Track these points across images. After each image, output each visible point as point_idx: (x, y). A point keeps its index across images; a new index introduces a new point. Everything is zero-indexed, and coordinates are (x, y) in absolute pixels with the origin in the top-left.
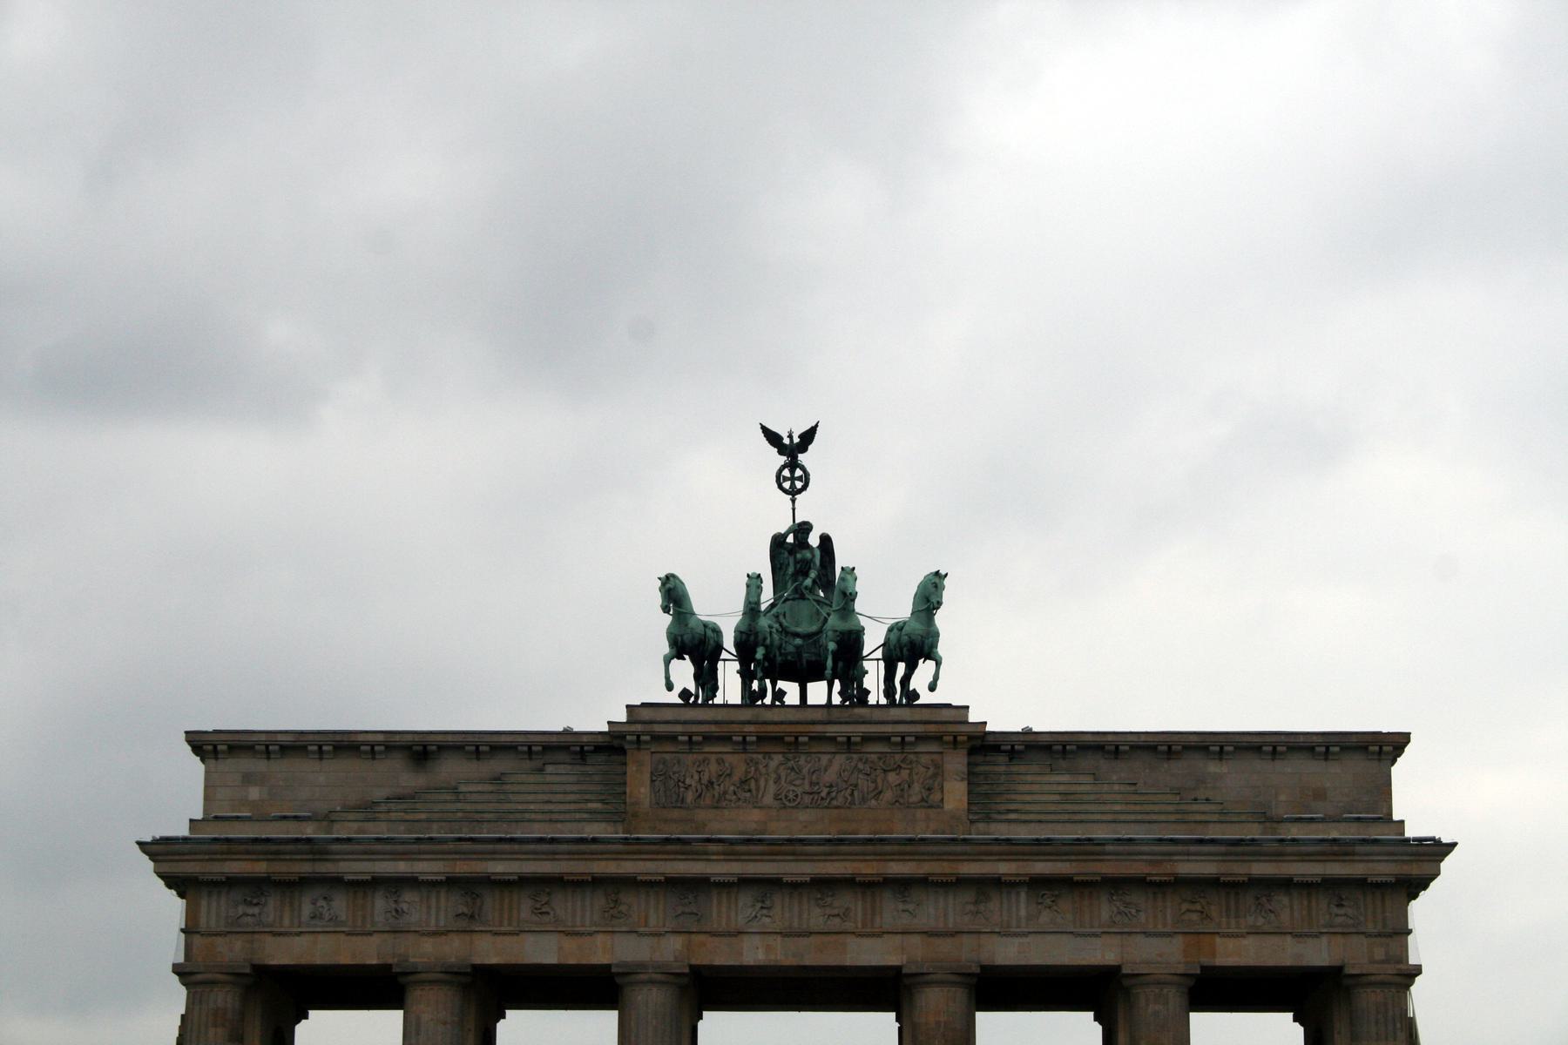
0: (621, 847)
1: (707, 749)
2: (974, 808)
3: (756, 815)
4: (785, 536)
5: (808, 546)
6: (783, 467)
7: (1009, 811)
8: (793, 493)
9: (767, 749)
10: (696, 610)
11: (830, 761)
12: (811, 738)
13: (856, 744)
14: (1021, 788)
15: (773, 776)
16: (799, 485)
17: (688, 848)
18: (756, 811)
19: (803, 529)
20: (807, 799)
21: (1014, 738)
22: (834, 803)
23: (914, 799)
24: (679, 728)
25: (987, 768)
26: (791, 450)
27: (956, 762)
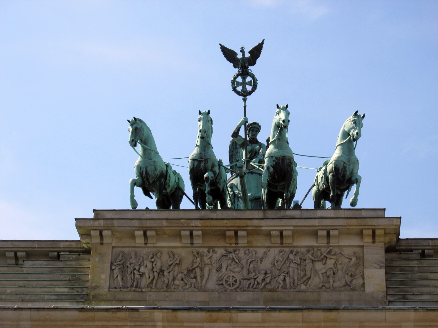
0: (77, 313)
2: (391, 292)
3: (201, 296)
4: (238, 129)
5: (256, 142)
6: (238, 75)
7: (422, 294)
8: (245, 94)
9: (212, 244)
10: (159, 150)
11: (265, 253)
13: (288, 236)
14: (432, 276)
15: (217, 265)
16: (249, 88)
17: (135, 314)
18: (199, 293)
19: (254, 128)
21: (425, 243)
22: (268, 287)
24: (136, 223)
26: (244, 63)
27: (375, 253)
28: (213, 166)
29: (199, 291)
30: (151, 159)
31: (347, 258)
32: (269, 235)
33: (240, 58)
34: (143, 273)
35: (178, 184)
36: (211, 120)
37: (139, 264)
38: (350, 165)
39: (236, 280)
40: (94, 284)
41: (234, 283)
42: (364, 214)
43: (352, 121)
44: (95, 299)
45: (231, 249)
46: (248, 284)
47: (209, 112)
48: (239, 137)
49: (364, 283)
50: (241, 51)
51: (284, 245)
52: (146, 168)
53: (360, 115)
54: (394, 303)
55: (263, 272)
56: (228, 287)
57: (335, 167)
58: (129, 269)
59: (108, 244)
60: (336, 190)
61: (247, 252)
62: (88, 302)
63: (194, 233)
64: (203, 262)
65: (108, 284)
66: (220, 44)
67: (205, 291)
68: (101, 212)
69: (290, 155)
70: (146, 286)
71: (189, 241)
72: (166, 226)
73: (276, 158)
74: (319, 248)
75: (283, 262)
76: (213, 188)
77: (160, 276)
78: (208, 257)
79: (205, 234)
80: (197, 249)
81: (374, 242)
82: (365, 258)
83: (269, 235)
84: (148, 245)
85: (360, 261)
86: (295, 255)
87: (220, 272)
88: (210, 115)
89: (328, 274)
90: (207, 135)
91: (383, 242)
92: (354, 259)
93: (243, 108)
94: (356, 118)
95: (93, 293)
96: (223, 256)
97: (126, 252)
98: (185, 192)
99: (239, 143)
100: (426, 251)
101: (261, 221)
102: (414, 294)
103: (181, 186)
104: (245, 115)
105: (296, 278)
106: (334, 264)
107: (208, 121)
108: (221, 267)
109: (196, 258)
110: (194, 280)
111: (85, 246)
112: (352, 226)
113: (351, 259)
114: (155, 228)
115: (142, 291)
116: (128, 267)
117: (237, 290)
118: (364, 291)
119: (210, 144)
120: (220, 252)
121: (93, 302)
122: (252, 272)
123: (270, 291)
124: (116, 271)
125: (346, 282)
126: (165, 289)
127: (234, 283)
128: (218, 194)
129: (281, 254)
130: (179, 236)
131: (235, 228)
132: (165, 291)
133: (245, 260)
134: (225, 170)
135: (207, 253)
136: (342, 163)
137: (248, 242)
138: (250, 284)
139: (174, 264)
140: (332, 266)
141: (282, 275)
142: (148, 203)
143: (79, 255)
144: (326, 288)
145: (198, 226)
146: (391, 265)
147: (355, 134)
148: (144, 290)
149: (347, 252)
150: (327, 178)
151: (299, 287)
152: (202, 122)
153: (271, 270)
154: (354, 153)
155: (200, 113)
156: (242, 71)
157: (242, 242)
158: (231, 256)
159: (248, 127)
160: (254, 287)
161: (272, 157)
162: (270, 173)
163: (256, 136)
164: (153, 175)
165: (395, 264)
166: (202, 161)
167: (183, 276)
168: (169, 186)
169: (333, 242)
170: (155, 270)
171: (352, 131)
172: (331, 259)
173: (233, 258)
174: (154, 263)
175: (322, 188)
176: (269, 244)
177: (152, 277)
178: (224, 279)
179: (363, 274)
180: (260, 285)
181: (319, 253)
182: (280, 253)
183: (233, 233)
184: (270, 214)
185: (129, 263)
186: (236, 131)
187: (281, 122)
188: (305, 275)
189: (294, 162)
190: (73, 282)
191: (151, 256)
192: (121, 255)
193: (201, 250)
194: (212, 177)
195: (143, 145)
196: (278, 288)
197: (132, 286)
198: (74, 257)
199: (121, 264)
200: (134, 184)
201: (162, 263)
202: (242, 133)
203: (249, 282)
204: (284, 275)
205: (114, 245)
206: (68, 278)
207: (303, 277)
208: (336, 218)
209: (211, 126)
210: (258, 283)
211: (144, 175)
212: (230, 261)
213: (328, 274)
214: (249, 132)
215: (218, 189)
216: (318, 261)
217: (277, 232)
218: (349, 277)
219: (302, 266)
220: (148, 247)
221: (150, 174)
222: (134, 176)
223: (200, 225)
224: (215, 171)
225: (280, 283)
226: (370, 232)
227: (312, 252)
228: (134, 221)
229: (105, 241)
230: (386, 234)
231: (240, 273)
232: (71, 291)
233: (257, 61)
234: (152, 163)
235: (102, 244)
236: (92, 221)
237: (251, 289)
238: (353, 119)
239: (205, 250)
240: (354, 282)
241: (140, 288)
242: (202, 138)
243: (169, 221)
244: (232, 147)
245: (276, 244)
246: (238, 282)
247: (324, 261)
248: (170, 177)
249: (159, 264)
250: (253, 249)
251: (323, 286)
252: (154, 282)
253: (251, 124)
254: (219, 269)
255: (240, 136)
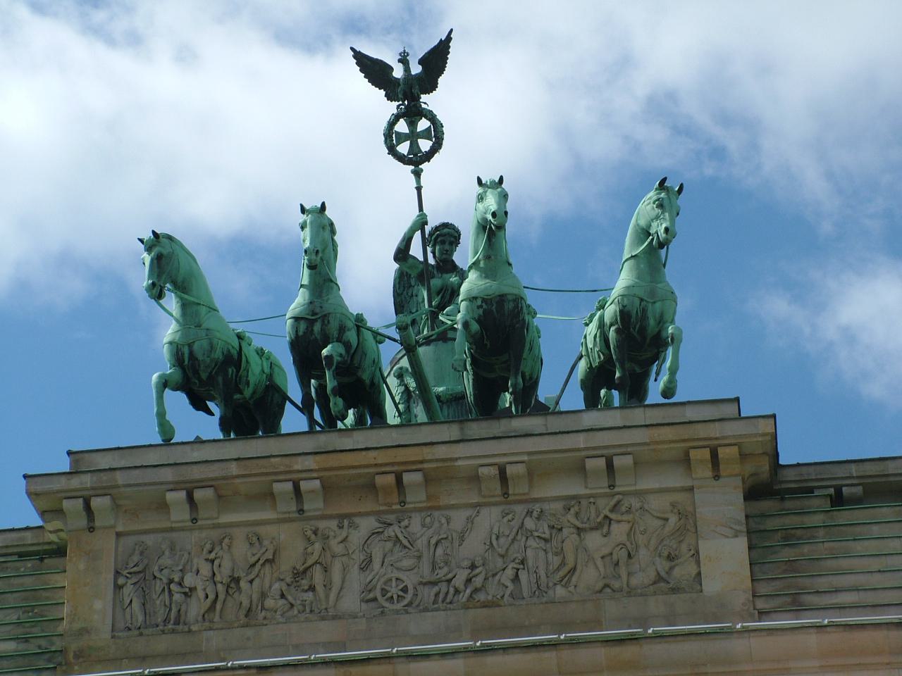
1: (226, 518)
2: (764, 589)
3: (326, 630)
4: (407, 241)
7: (837, 591)
8: (416, 160)
11: (470, 520)
12: (428, 480)
14: (859, 547)
15: (359, 557)
16: (425, 145)
19: (446, 237)
20: (428, 594)
21: (840, 472)
22: (481, 597)
23: (641, 578)
24: (168, 475)
25: (789, 521)
26: (409, 87)
27: (722, 503)
28: (342, 329)
29: (323, 619)
30: (199, 326)
31: (658, 518)
32: (474, 479)
33: (399, 77)
34: (191, 589)
35: (270, 377)
36: (332, 224)
37: (180, 568)
38: (654, 302)
39: (406, 586)
40: (77, 626)
41: (401, 593)
42: (691, 413)
43: (654, 203)
44: (81, 660)
45: (391, 518)
46: (433, 594)
47: (323, 204)
48: (410, 261)
49: (699, 574)
50: (400, 61)
51: (511, 498)
52: (190, 346)
53: (672, 188)
54: (774, 616)
55: (466, 563)
56: (387, 604)
57: (621, 312)
58: (158, 581)
59: (105, 528)
60: (628, 365)
61: (428, 520)
62: (64, 668)
63: (304, 485)
64: (328, 554)
65: (109, 621)
66: (352, 49)
67: (335, 618)
68: (86, 455)
69: (515, 291)
70: (200, 618)
71: (294, 509)
72: (237, 477)
73: (484, 300)
74: (592, 500)
75: (511, 537)
76: (346, 380)
77: (231, 591)
78: (340, 539)
79: (328, 489)
80: (312, 522)
81: (717, 477)
82: (697, 515)
83: (474, 479)
84: (199, 523)
85: (688, 523)
86: (538, 519)
87: (368, 572)
88: (326, 212)
89: (615, 557)
90: (322, 259)
91: (736, 475)
92: (673, 519)
93: (416, 191)
94: (663, 195)
95: (74, 647)
96: (373, 534)
97: (150, 543)
98: (289, 395)
99: (414, 273)
100: (844, 489)
101: (454, 446)
102: (818, 592)
103: (278, 380)
104: (421, 208)
105: (542, 573)
106: (628, 535)
107: (323, 228)
108: (371, 561)
109: (313, 544)
110: (310, 594)
111: (53, 538)
112: (663, 442)
113: (667, 520)
114: (211, 483)
115: (190, 631)
116: (155, 577)
117: (410, 610)
118: (701, 591)
119: (331, 281)
120: (367, 525)
121: (76, 668)
122: (442, 565)
123: (485, 605)
124: (128, 590)
125: (658, 574)
126: (243, 620)
127: (401, 593)
128: (361, 392)
129: (505, 519)
130: (268, 496)
131: (396, 468)
132: (242, 627)
133: (425, 539)
134: (375, 338)
135: (336, 528)
136: (637, 302)
137: (429, 498)
138: (437, 595)
139: (261, 562)
140: (623, 538)
141: (510, 567)
142: (199, 425)
143: (42, 560)
144: (614, 591)
145: (311, 470)
146: (762, 527)
147: (662, 231)
148: (194, 628)
149: (657, 503)
150: (605, 340)
151: (551, 592)
152: (308, 230)
153: (484, 559)
154: (664, 274)
155: (303, 210)
156: (406, 107)
157: (416, 497)
158: (390, 532)
159: (431, 235)
160: (448, 600)
161: (475, 298)
162: (472, 336)
163: (451, 254)
164: (208, 360)
165: (771, 524)
166: (316, 320)
167: (284, 588)
168: (248, 383)
169: (623, 485)
170: (218, 578)
171: (654, 224)
172: (619, 522)
173: (397, 537)
174: (216, 562)
175: (597, 360)
176: (475, 500)
177: (212, 597)
178: (378, 587)
179: (697, 552)
180: (462, 594)
181: (593, 508)
182: (503, 517)
183: (391, 479)
184: (477, 428)
185: (156, 568)
186: (402, 248)
187: (490, 217)
188: (563, 564)
189: (529, 306)
190: (28, 625)
191: (208, 546)
192: (137, 552)
193: (322, 525)
194: (341, 355)
195: (178, 293)
196: (503, 597)
197: (166, 621)
198: (29, 565)
199: (139, 572)
200: (164, 384)
201: (233, 561)
202: (416, 250)
203: (436, 589)
204: (515, 566)
205: (120, 529)
206: (16, 617)
207: (558, 569)
208: (625, 427)
209: (333, 239)
210: (457, 591)
211: (186, 362)
212: (389, 545)
213: (615, 557)
214: (434, 246)
215: (360, 381)
216: (592, 529)
217: (491, 468)
218: (664, 562)
219: (554, 543)
220: (201, 528)
221: (200, 358)
222: (166, 367)
223: (314, 466)
224: (349, 342)
225: (507, 587)
226: (706, 454)
227: (576, 508)
228: (163, 470)
229: (97, 523)
230: (743, 456)
231: (415, 571)
232: (22, 646)
233: (440, 80)
234: (203, 333)
235: (91, 529)
236: (63, 479)
237: (440, 605)
238: (655, 198)
239: (333, 524)
240: (677, 572)
241: (185, 624)
242: (312, 267)
243: (243, 463)
244: (399, 283)
245: (493, 496)
246: (411, 591)
247: (605, 530)
248: (247, 361)
249: (227, 564)
250: (444, 512)
251: (607, 586)
252: (218, 607)
253: (437, 228)
254: (366, 565)
255: (414, 258)
